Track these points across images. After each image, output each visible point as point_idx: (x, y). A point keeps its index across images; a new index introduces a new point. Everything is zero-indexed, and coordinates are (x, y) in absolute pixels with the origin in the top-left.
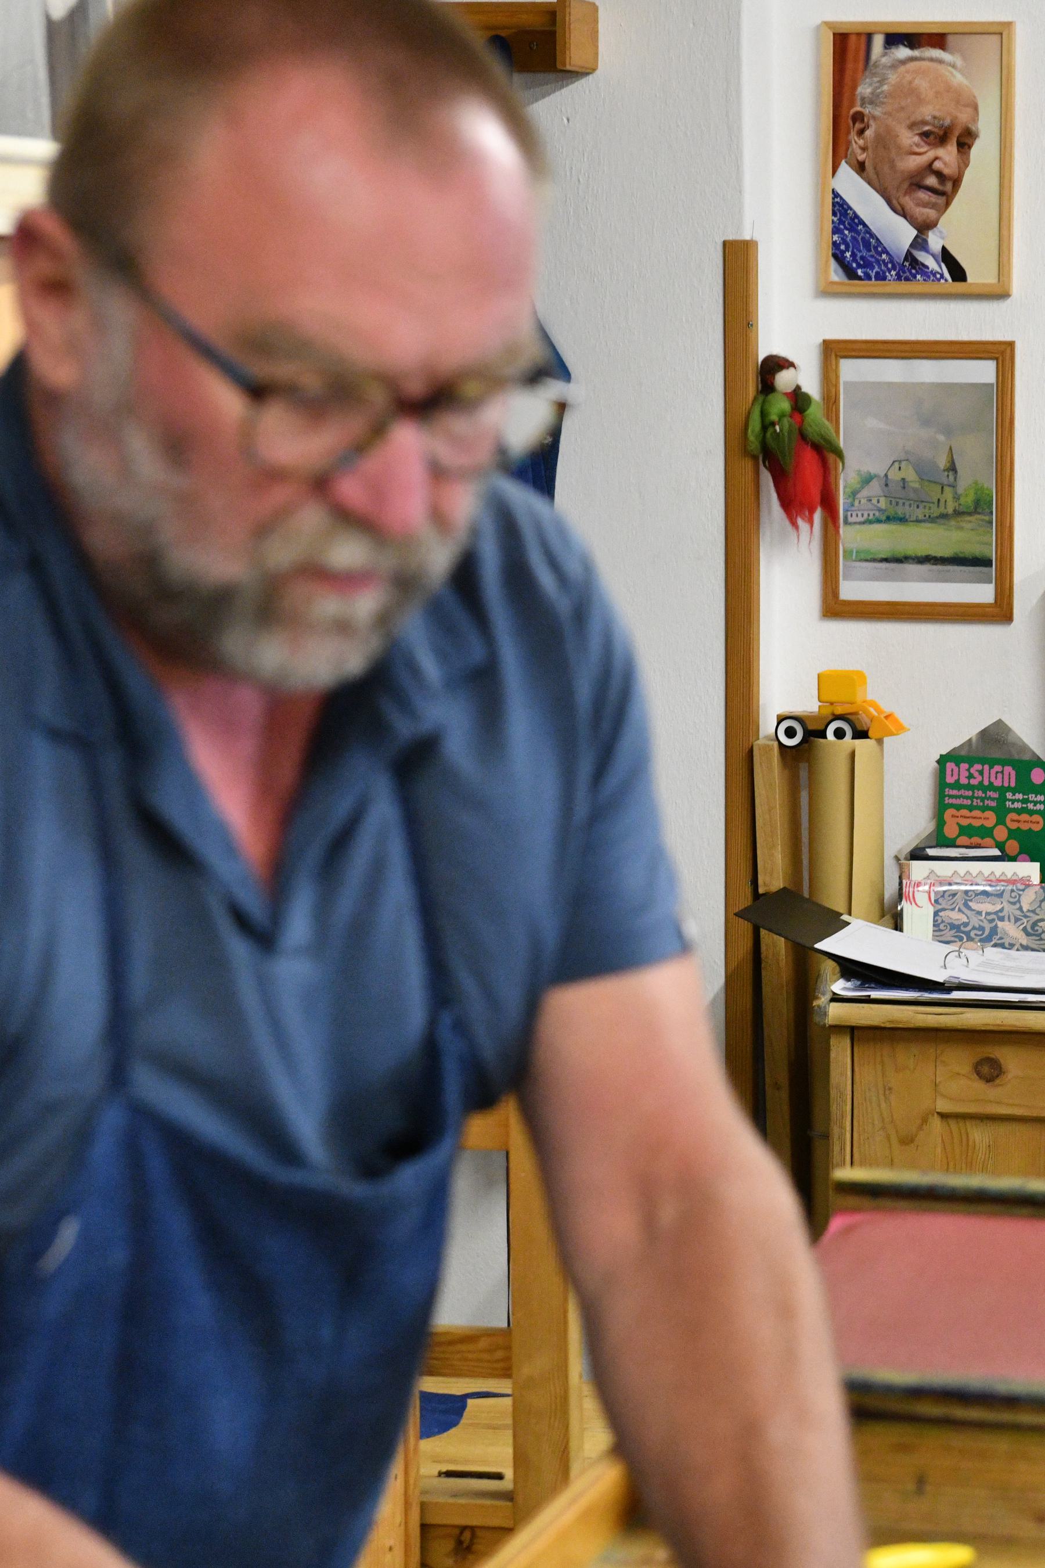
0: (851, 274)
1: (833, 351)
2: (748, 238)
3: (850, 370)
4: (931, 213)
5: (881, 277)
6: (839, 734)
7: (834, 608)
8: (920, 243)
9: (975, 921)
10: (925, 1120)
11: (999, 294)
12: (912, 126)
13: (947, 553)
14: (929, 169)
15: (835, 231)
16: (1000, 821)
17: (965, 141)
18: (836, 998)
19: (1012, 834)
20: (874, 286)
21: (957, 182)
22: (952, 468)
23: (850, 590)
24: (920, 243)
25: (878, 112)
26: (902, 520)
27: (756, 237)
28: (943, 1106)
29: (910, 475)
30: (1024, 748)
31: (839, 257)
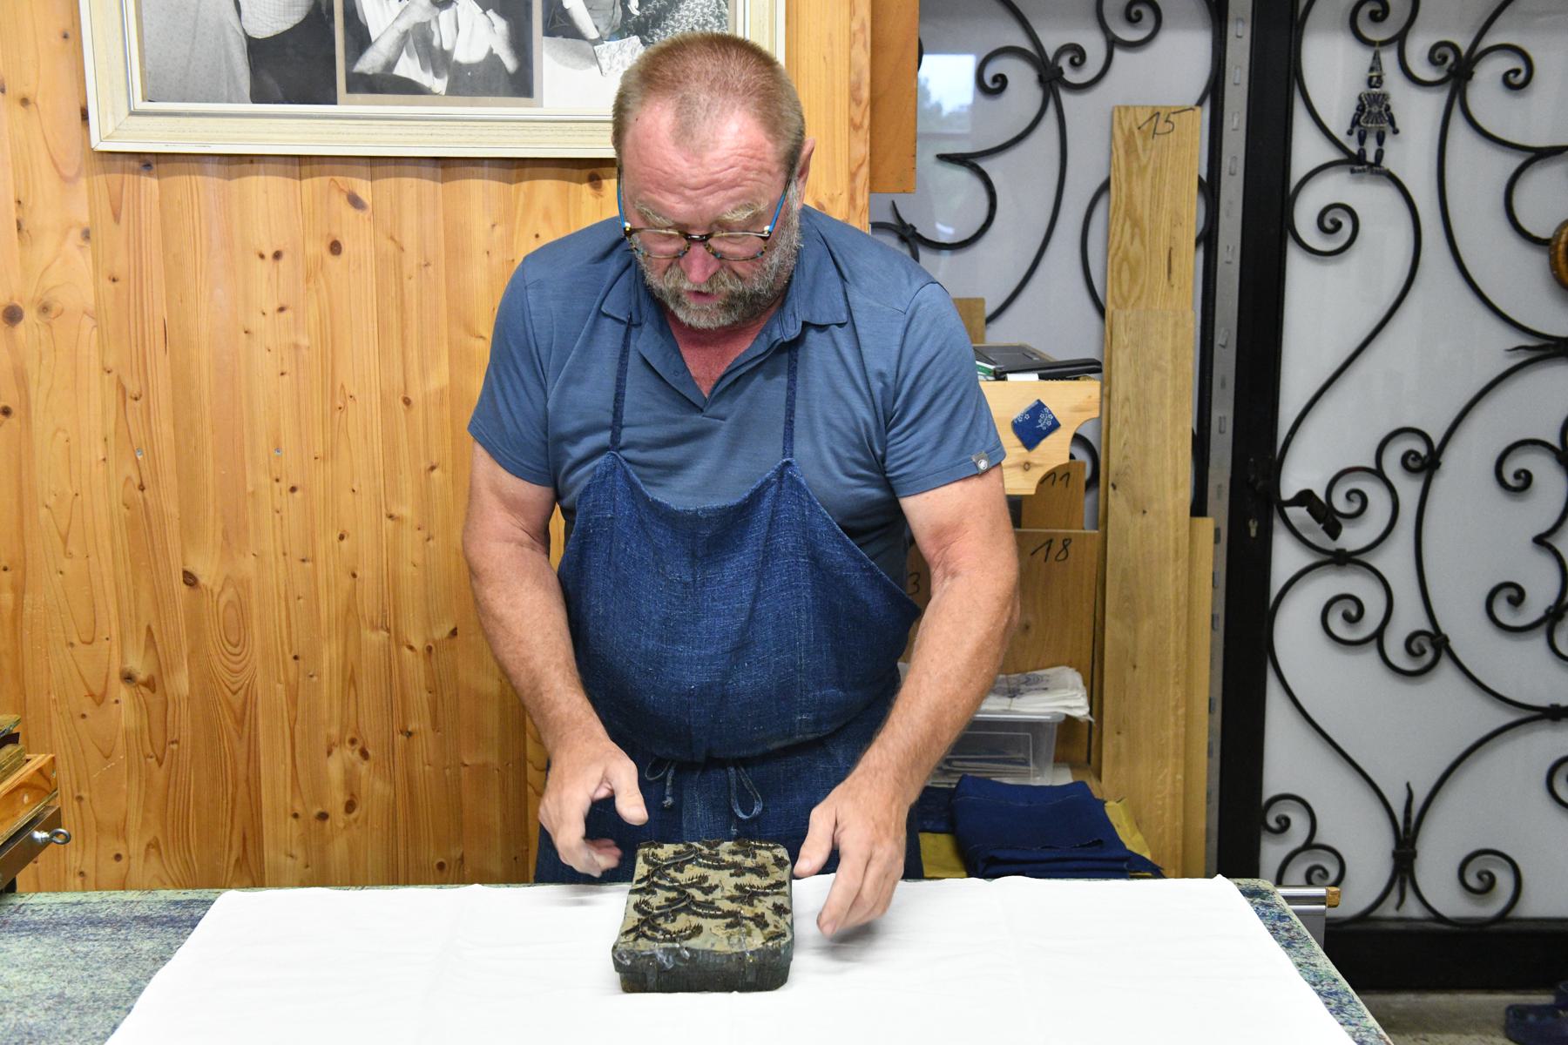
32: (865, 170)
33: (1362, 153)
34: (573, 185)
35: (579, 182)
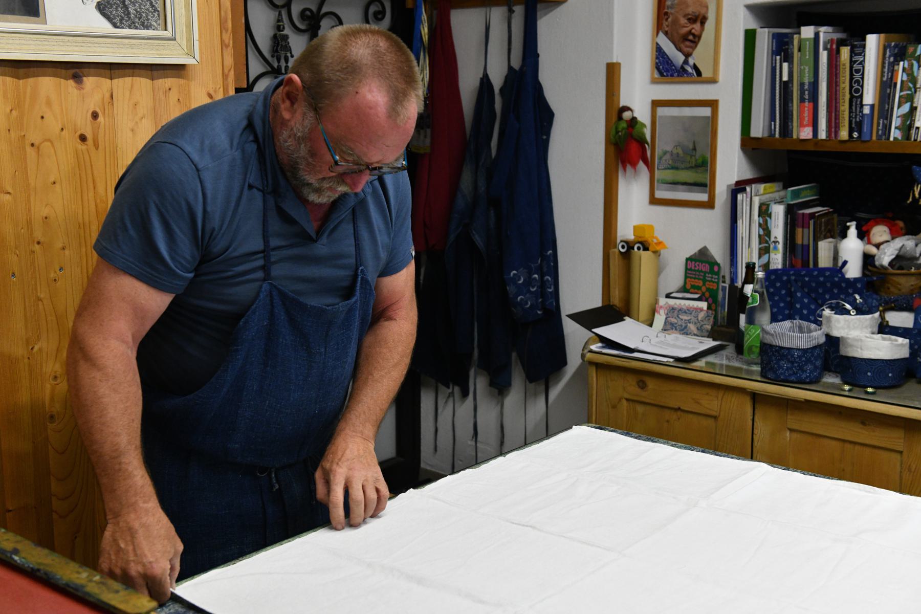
0: (661, 74)
1: (656, 104)
2: (615, 61)
3: (662, 111)
4: (689, 50)
5: (672, 76)
6: (639, 248)
7: (654, 201)
8: (686, 62)
9: (680, 323)
10: (620, 400)
11: (713, 81)
12: (685, 16)
13: (691, 181)
14: (690, 33)
15: (657, 58)
16: (704, 284)
17: (703, 20)
18: (591, 351)
19: (708, 289)
20: (669, 79)
21: (699, 37)
22: (694, 149)
23: (659, 194)
24: (686, 62)
25: (673, 11)
26: (677, 168)
27: (619, 61)
28: (626, 396)
29: (680, 151)
30: (712, 257)
31: (658, 68)
32: (232, 72)
33: (279, 67)
34: (62, 80)
35: (66, 79)
